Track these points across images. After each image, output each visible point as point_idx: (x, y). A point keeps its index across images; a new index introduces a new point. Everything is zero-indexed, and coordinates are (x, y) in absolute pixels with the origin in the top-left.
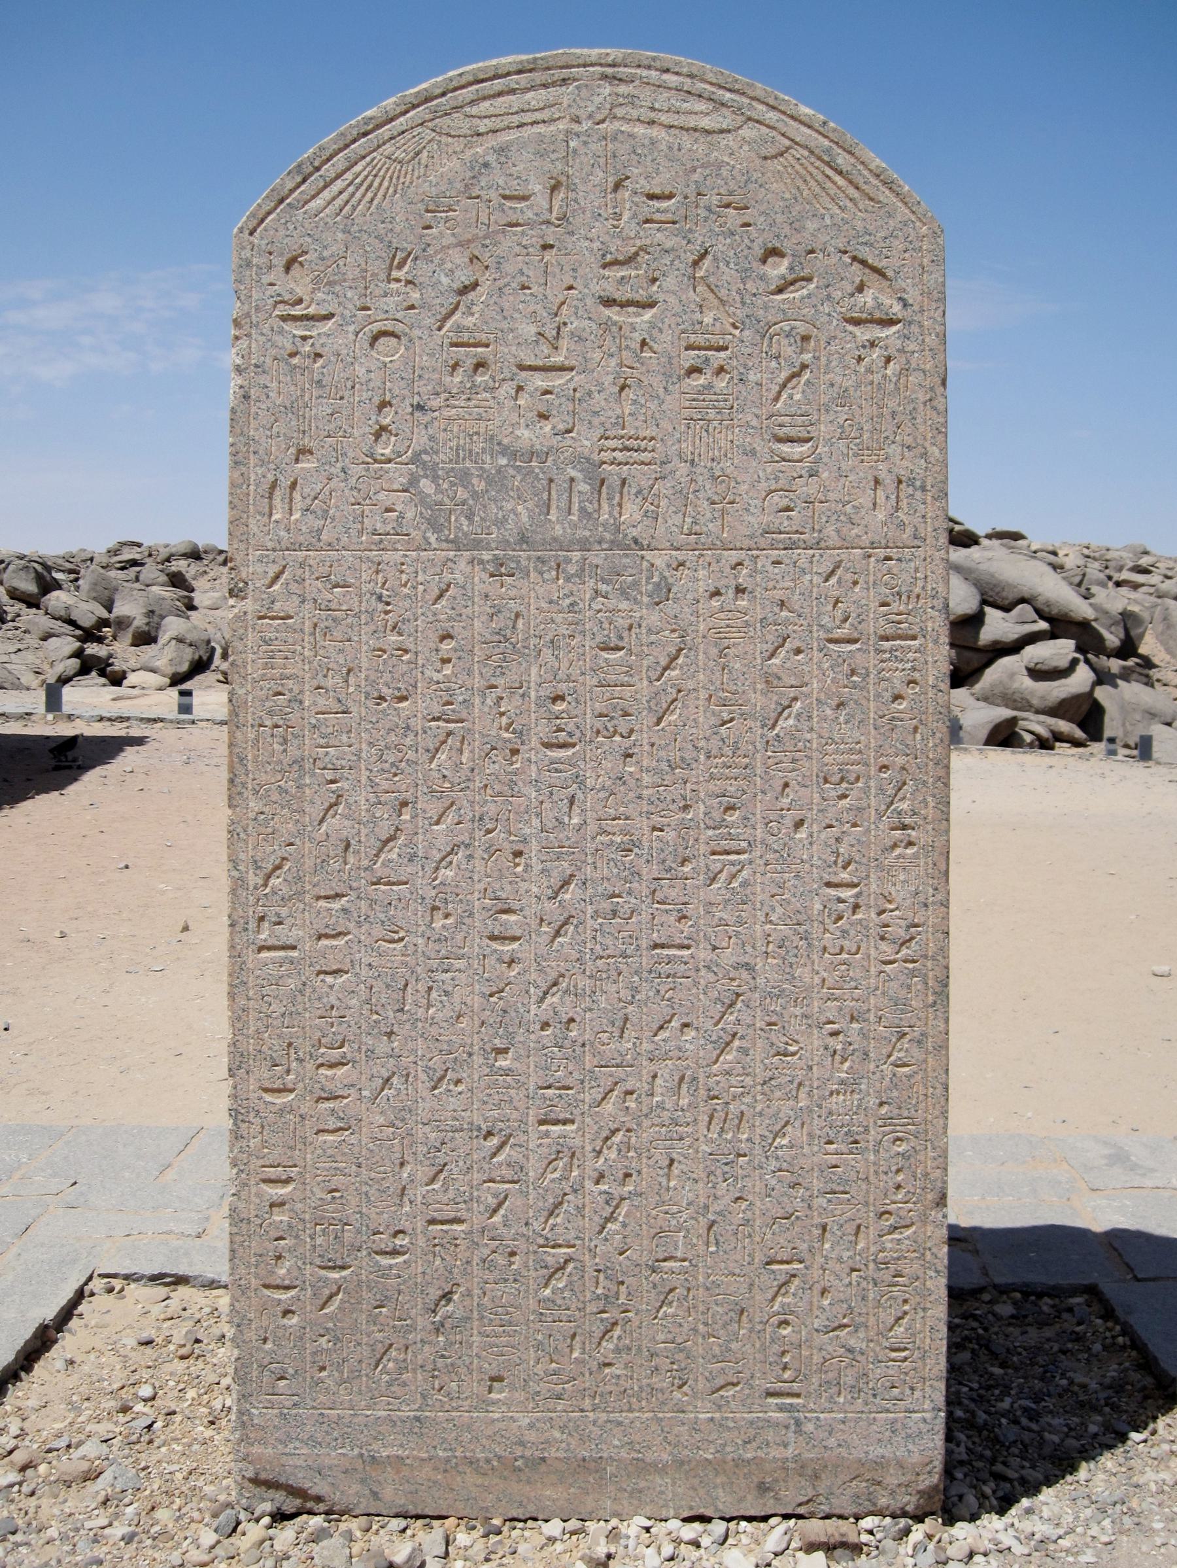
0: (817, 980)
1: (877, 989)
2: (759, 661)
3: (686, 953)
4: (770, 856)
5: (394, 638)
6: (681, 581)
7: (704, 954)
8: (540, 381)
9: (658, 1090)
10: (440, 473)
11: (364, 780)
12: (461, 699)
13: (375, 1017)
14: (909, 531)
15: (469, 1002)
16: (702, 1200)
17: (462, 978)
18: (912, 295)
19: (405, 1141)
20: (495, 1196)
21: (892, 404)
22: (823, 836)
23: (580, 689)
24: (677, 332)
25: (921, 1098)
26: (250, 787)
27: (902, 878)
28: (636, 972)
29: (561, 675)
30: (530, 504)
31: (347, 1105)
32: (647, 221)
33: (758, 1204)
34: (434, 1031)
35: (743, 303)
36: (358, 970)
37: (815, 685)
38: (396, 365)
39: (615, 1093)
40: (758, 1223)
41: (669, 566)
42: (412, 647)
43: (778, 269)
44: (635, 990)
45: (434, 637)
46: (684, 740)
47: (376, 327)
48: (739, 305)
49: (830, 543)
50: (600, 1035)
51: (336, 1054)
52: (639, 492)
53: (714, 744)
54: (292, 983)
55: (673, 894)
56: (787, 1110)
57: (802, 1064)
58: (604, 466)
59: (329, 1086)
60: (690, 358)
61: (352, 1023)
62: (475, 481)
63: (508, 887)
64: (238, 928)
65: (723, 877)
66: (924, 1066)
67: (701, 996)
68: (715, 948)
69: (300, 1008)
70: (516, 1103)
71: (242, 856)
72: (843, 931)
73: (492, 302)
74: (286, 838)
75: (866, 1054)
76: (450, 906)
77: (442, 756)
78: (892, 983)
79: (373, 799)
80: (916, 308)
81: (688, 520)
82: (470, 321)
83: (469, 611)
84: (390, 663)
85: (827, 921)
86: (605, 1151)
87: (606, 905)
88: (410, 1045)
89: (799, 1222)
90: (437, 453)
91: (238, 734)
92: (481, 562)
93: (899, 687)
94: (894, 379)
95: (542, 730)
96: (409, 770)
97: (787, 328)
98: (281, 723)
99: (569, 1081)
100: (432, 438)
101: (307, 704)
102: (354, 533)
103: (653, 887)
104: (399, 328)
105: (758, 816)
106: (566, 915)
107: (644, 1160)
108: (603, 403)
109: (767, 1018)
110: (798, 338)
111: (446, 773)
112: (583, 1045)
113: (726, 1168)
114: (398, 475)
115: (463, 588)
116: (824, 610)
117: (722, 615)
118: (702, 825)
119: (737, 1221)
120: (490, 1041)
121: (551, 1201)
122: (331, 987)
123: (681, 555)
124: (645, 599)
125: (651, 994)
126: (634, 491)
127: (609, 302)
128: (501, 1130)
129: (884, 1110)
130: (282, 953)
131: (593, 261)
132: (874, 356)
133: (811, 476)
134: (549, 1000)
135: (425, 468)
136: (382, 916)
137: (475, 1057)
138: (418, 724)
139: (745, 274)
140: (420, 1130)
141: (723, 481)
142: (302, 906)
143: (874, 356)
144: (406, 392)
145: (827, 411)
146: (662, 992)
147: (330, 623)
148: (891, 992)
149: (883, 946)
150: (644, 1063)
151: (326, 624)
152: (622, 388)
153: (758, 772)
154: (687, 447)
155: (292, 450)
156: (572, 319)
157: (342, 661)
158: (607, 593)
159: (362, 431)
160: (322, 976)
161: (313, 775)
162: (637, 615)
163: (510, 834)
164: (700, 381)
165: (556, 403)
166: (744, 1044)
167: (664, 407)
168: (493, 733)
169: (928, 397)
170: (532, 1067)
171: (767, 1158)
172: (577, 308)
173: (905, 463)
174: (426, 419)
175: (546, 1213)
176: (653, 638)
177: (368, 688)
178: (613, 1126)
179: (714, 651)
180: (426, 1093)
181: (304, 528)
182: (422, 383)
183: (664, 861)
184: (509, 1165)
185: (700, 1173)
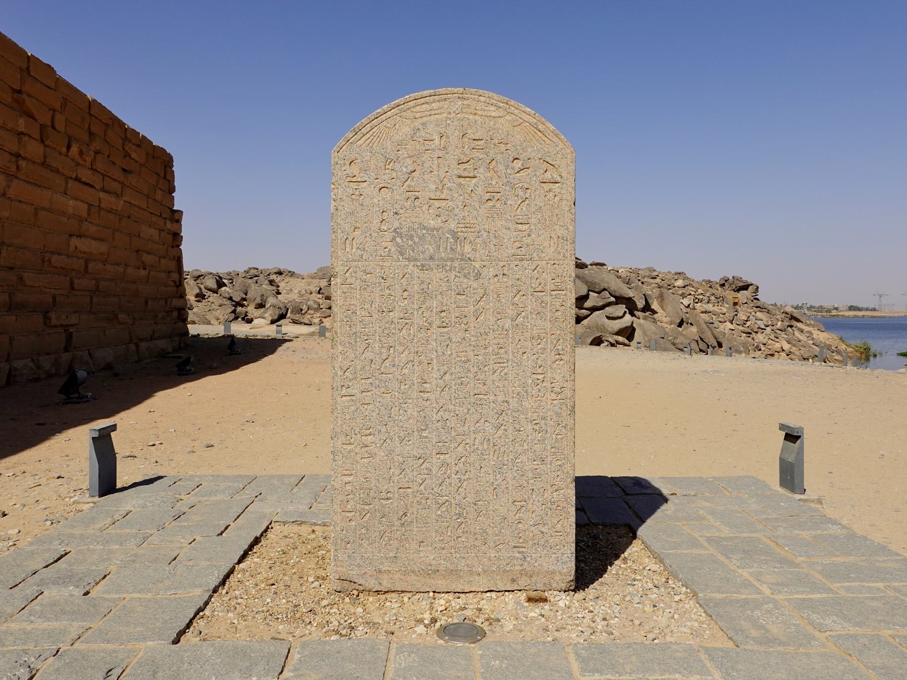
5: (388, 291)
6: (484, 272)
7: (492, 398)
8: (437, 204)
17: (410, 406)
18: (564, 174)
21: (556, 211)
34: (401, 424)
43: (518, 165)
44: (469, 410)
47: (381, 186)
51: (368, 432)
53: (495, 327)
54: (353, 408)
56: (520, 449)
60: (488, 196)
82: (413, 184)
87: (459, 381)
93: (558, 308)
95: (438, 323)
104: (389, 186)
114: (388, 236)
123: (484, 263)
127: (460, 177)
131: (455, 163)
138: (396, 321)
139: (507, 167)
140: (396, 458)
149: (553, 394)
154: (486, 227)
159: (376, 221)
164: (491, 204)
179: (495, 296)
185: (491, 472)
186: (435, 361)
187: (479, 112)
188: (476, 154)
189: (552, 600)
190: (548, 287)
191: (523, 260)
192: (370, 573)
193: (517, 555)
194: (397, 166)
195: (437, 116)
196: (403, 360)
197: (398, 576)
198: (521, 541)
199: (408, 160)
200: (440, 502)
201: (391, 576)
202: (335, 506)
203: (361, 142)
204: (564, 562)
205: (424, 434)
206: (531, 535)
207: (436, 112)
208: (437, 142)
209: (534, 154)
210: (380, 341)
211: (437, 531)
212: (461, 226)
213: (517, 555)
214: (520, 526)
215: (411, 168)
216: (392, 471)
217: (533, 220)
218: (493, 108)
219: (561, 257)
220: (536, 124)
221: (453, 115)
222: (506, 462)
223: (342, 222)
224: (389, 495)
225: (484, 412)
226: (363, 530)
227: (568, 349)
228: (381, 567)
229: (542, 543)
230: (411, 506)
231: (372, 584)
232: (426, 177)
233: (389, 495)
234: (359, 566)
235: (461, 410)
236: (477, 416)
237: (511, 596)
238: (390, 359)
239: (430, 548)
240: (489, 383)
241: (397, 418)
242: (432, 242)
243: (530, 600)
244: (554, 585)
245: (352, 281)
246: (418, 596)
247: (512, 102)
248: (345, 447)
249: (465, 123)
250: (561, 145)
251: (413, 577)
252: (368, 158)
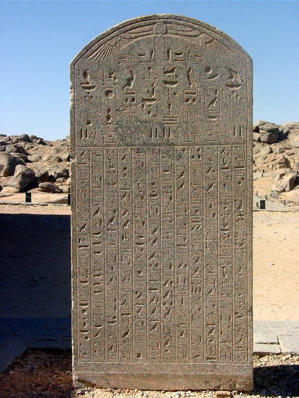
8: (148, 103)
35: (200, 81)
55: (182, 232)
60: (186, 96)
62: (132, 129)
95: (149, 192)
99: (157, 279)
100: (121, 118)
104: (112, 89)
122: (97, 256)
123: (184, 147)
127: (166, 82)
195: (148, 36)
245: (86, 161)
251: (133, 379)
252: (96, 69)
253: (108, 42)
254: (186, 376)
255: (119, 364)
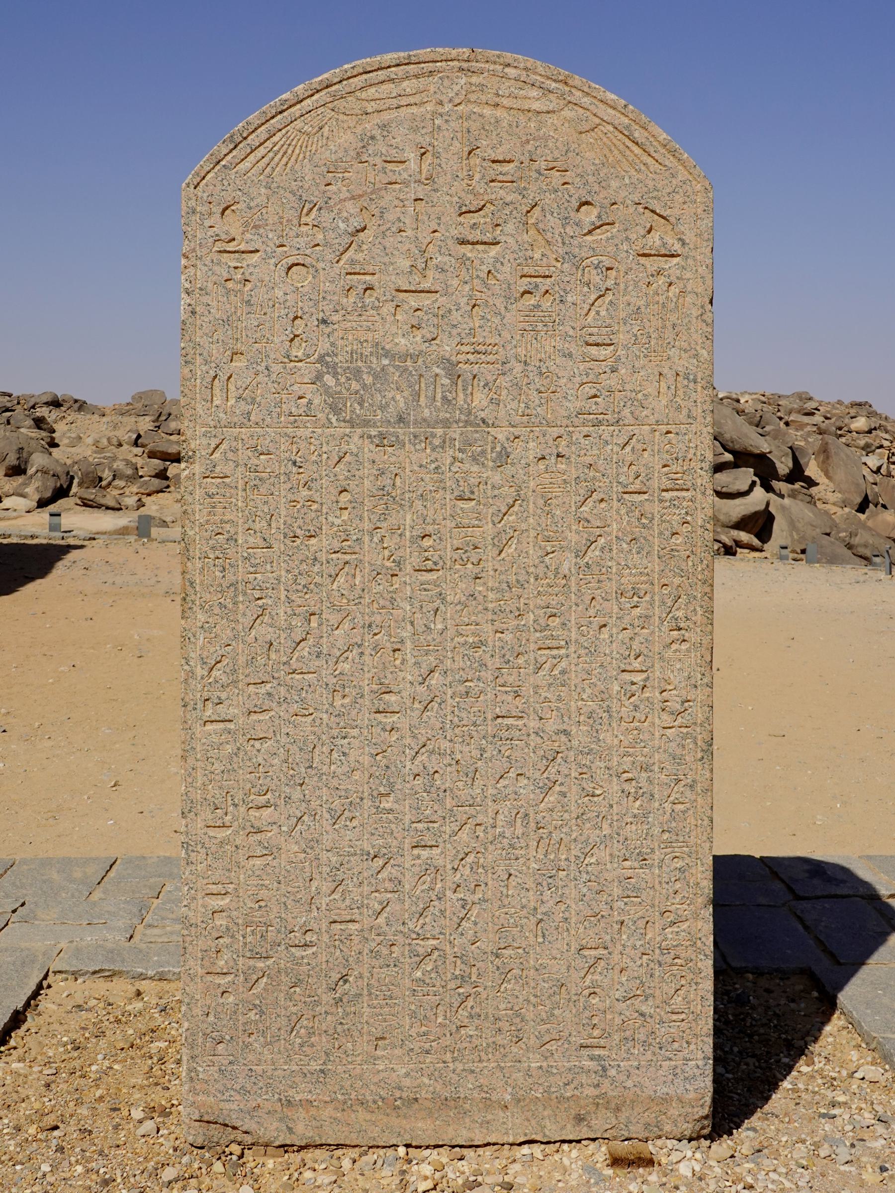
0: (616, 742)
1: (660, 748)
2: (574, 509)
3: (520, 723)
4: (582, 652)
5: (305, 493)
6: (516, 450)
7: (533, 724)
8: (413, 301)
9: (499, 823)
10: (339, 370)
11: (283, 597)
12: (355, 538)
13: (292, 772)
14: (685, 412)
15: (361, 761)
16: (532, 904)
17: (356, 743)
18: (689, 237)
19: (314, 864)
20: (380, 903)
21: (673, 318)
22: (620, 636)
23: (442, 530)
24: (515, 265)
25: (693, 827)
26: (198, 603)
27: (678, 666)
28: (484, 737)
29: (428, 520)
30: (406, 394)
31: (271, 838)
32: (493, 181)
33: (574, 906)
34: (335, 783)
35: (564, 243)
36: (279, 738)
37: (615, 526)
38: (305, 289)
39: (468, 826)
40: (573, 920)
41: (508, 439)
42: (318, 499)
43: (589, 216)
44: (483, 750)
45: (335, 492)
46: (519, 567)
47: (291, 260)
48: (560, 245)
49: (626, 422)
50: (457, 784)
51: (262, 800)
52: (486, 384)
53: (541, 570)
54: (229, 748)
55: (511, 679)
56: (594, 836)
57: (605, 803)
58: (460, 365)
59: (257, 824)
61: (274, 777)
62: (365, 376)
63: (389, 676)
64: (189, 708)
65: (547, 666)
66: (695, 804)
67: (532, 755)
68: (541, 719)
69: (236, 766)
70: (395, 834)
71: (192, 655)
72: (635, 706)
73: (377, 242)
74: (225, 641)
75: (652, 795)
76: (347, 690)
77: (341, 579)
78: (671, 744)
79: (290, 612)
80: (691, 246)
81: (523, 405)
82: (360, 257)
83: (360, 473)
84: (302, 511)
85: (623, 698)
86: (460, 867)
87: (461, 689)
88: (318, 793)
89: (604, 920)
90: (336, 355)
91: (189, 564)
92: (370, 437)
93: (677, 527)
94: (674, 300)
96: (316, 590)
97: (596, 262)
98: (221, 556)
99: (434, 818)
100: (333, 344)
101: (240, 541)
102: (275, 415)
103: (496, 675)
104: (308, 261)
105: (573, 622)
106: (432, 696)
107: (490, 875)
108: (460, 318)
109: (580, 770)
110: (604, 269)
111: (344, 592)
112: (445, 791)
113: (550, 881)
114: (307, 371)
115: (356, 455)
116: (621, 471)
117: (547, 476)
118: (532, 630)
119: (557, 920)
120: (377, 789)
121: (422, 906)
122: (258, 751)
124: (491, 464)
125: (495, 753)
126: (482, 384)
127: (463, 242)
128: (385, 854)
129: (666, 836)
130: (221, 725)
131: (453, 211)
132: (660, 283)
133: (613, 372)
134: (420, 758)
135: (327, 367)
136: (296, 698)
137: (365, 801)
138: (322, 556)
139: (566, 221)
140: (324, 856)
141: (548, 376)
142: (237, 691)
143: (660, 283)
144: (313, 310)
145: (625, 324)
146: (503, 752)
147: (257, 482)
148: (670, 750)
149: (665, 716)
150: (490, 804)
151: (255, 483)
152: (474, 307)
153: (573, 589)
154: (521, 351)
155: (229, 353)
156: (437, 255)
157: (266, 510)
158: (462, 459)
159: (280, 339)
160: (252, 742)
161: (245, 594)
162: (485, 475)
163: (390, 635)
164: (531, 301)
165: (426, 318)
166: (563, 789)
167: (505, 321)
168: (379, 563)
169: (699, 313)
170: (407, 807)
171: (580, 872)
172: (440, 247)
173: (682, 362)
174: (328, 330)
175: (418, 915)
176: (496, 492)
177: (286, 530)
178: (467, 850)
179: (541, 502)
180: (329, 828)
181: (237, 411)
182: (325, 303)
183: (504, 656)
184: (390, 880)
185: (530, 884)
186: (409, 644)
187: (505, 102)
188: (499, 192)
189: (664, 1161)
190: (655, 484)
191: (598, 424)
192: (268, 1106)
193: (587, 1063)
194: (326, 217)
195: (414, 110)
196: (339, 644)
197: (328, 1112)
198: (596, 1033)
199: (349, 205)
200: (421, 951)
201: (313, 1111)
202: (191, 963)
203: (247, 164)
204: (691, 1076)
205: (386, 805)
206: (618, 1021)
207: (412, 100)
208: (413, 165)
209: (623, 194)
210: (290, 601)
211: (413, 1014)
212: (465, 349)
213: (587, 1063)
214: (595, 1001)
215: (356, 223)
216: (315, 884)
217: (622, 338)
218: (534, 93)
219: (682, 417)
220: (627, 127)
221: (448, 107)
222: (563, 864)
223: (204, 341)
224: (309, 937)
225: (517, 754)
226: (252, 1015)
227: (698, 618)
228: (291, 1092)
229: (642, 1037)
230: (358, 961)
231: (272, 1129)
232: (389, 242)
233: (309, 937)
234: (243, 1091)
235: (466, 752)
236: (501, 765)
237: (574, 1153)
238: (311, 641)
239: (398, 1052)
240: (527, 690)
241: (325, 769)
242: (404, 386)
243: (616, 1161)
244: (667, 1128)
245: (228, 469)
246: (372, 1156)
247: (577, 80)
248: (211, 832)
249: (474, 126)
250: (682, 174)
251: (362, 1114)
253: (299, 124)
254: (519, 1101)
255: (322, 1071)
